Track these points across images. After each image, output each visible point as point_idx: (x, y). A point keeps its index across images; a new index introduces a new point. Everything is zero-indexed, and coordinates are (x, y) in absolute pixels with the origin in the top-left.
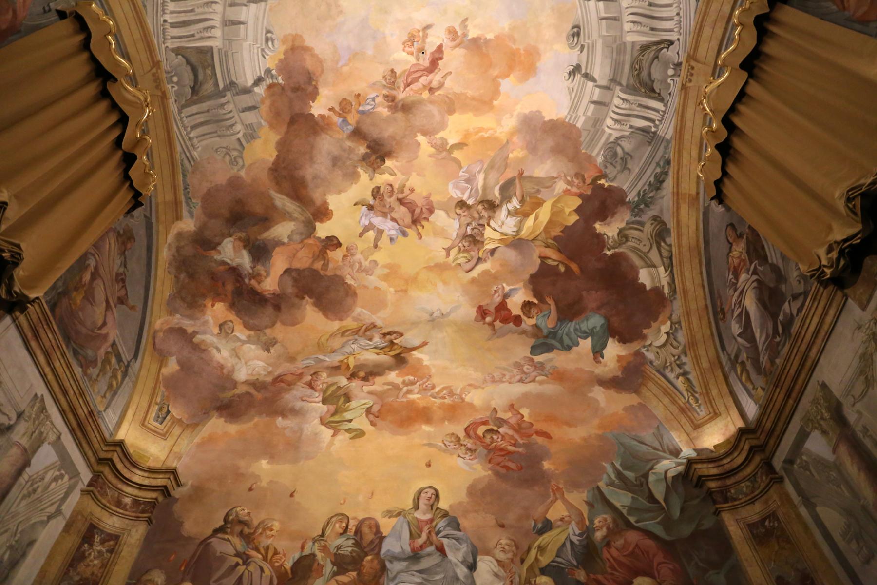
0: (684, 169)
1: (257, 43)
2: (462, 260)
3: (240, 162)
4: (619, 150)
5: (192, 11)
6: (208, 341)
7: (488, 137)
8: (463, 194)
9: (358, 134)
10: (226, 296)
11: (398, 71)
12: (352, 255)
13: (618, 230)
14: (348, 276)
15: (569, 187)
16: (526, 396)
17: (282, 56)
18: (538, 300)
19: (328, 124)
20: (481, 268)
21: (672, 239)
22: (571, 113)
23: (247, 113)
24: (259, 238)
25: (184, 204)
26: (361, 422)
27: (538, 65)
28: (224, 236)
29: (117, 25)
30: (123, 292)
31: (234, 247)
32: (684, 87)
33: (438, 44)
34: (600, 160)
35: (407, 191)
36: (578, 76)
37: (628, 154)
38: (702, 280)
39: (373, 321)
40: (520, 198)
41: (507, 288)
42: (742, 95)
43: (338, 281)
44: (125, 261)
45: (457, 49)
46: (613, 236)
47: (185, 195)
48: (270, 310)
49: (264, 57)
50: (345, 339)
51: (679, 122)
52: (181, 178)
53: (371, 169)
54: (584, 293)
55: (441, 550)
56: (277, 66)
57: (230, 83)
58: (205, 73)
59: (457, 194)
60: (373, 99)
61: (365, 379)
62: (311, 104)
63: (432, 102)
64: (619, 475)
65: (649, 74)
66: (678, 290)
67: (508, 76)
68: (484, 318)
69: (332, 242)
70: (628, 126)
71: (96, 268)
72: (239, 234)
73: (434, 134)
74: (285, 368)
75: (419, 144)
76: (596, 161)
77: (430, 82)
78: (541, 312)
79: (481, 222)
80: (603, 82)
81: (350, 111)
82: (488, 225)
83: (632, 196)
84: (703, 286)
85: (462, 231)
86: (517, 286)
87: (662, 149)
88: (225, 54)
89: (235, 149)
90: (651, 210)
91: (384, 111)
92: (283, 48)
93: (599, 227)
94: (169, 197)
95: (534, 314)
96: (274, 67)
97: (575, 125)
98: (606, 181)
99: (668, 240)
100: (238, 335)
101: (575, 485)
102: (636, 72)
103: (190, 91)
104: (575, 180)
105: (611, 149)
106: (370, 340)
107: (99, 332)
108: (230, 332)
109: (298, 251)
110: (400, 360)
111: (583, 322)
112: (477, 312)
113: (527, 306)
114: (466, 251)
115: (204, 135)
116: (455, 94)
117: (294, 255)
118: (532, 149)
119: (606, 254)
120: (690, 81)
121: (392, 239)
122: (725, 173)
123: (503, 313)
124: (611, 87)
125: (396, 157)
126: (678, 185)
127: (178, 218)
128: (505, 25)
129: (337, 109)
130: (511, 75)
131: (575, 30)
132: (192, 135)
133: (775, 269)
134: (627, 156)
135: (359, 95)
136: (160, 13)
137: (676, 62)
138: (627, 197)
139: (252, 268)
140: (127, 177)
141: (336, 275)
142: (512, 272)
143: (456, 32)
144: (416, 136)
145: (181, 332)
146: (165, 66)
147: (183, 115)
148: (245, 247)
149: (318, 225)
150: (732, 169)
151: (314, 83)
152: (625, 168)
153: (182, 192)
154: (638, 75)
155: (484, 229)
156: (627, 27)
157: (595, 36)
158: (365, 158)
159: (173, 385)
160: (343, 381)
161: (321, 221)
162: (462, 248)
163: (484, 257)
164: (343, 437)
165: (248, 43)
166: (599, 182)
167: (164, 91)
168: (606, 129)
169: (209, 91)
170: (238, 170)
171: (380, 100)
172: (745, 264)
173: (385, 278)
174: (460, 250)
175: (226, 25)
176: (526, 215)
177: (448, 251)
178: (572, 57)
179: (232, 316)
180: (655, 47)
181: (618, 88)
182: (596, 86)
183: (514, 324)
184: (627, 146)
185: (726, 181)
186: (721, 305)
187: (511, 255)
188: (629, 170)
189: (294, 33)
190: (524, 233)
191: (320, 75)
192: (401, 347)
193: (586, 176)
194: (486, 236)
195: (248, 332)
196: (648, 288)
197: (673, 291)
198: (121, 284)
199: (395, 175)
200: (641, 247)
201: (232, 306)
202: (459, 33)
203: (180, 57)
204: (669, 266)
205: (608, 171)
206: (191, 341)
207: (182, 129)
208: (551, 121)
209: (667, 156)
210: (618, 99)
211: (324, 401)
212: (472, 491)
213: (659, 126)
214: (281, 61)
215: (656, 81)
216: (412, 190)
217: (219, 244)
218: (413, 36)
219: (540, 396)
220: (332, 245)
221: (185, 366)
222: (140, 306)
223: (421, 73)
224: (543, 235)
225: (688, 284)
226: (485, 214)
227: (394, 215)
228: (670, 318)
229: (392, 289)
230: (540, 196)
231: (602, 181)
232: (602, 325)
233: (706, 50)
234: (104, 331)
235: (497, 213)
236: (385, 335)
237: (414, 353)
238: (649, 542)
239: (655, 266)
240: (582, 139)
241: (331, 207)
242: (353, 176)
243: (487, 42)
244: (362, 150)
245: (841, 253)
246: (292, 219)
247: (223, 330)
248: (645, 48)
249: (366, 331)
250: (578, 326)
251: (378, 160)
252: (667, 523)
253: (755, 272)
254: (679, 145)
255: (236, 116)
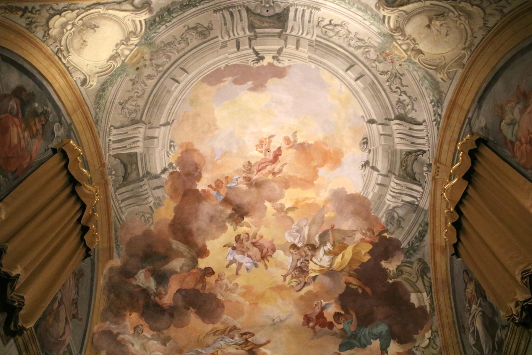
0: (437, 229)
1: (164, 148)
2: (294, 284)
3: (151, 220)
4: (395, 215)
5: (126, 133)
6: (126, 339)
7: (311, 204)
8: (295, 239)
9: (227, 201)
10: (139, 308)
11: (253, 162)
12: (222, 280)
13: (396, 267)
14: (219, 294)
15: (364, 237)
17: (179, 155)
18: (344, 311)
19: (207, 195)
20: (306, 289)
21: (431, 275)
22: (364, 190)
23: (157, 190)
24: (161, 269)
25: (115, 249)
27: (342, 160)
28: (139, 269)
29: (83, 151)
30: (75, 312)
31: (145, 276)
32: (434, 179)
33: (279, 146)
34: (383, 220)
35: (258, 238)
36: (368, 168)
37: (401, 217)
38: (451, 304)
39: (235, 324)
40: (332, 243)
41: (324, 303)
42: (465, 194)
43: (212, 297)
44: (78, 290)
45: (291, 149)
46: (393, 271)
47: (116, 243)
48: (166, 317)
49: (168, 156)
50: (216, 337)
51: (432, 200)
52: (114, 233)
53: (234, 223)
54: (375, 308)
56: (176, 161)
57: (147, 173)
58: (131, 169)
59: (290, 240)
60: (237, 180)
62: (197, 183)
63: (274, 181)
65: (412, 170)
66: (435, 309)
67: (323, 166)
68: (308, 323)
69: (209, 271)
70: (400, 200)
71: (61, 298)
72: (148, 267)
73: (276, 201)
75: (266, 208)
76: (381, 220)
77: (274, 169)
78: (347, 320)
79: (307, 258)
80: (384, 172)
81: (222, 187)
82: (311, 260)
83: (404, 245)
84: (452, 308)
85: (294, 264)
86: (330, 302)
87: (422, 216)
88: (144, 156)
89: (148, 213)
90: (418, 254)
91: (244, 187)
92: (180, 151)
93: (383, 264)
94: (106, 245)
95: (342, 322)
96: (174, 162)
97: (367, 198)
98: (388, 234)
99: (428, 275)
100: (145, 333)
102: (404, 168)
103: (122, 178)
104: (368, 233)
105: (391, 213)
106: (233, 338)
107: (60, 339)
108: (140, 332)
109: (186, 277)
111: (374, 327)
112: (304, 319)
113: (337, 315)
114: (296, 277)
115: (129, 205)
116: (289, 176)
117: (184, 280)
118: (340, 211)
119: (388, 282)
120: (438, 175)
121: (248, 269)
122: (459, 240)
123: (321, 320)
124: (389, 175)
125: (251, 216)
126: (434, 240)
127: (111, 258)
128: (320, 136)
129: (214, 186)
130: (325, 166)
131: (365, 140)
132: (121, 205)
133: (491, 306)
134: (400, 219)
135: (227, 177)
136: (107, 135)
137: (428, 163)
138: (401, 245)
139: (156, 289)
140: (82, 240)
141: (211, 294)
142: (328, 292)
143: (290, 140)
144: (264, 202)
145: (109, 333)
146: (108, 166)
147: (117, 193)
148: (152, 275)
149: (199, 260)
150: (462, 238)
151: (199, 170)
152: (399, 226)
153: (114, 241)
154: (405, 169)
155: (309, 263)
156: (397, 140)
157: (377, 144)
158: (231, 217)
161: (202, 257)
162: (294, 276)
163: (308, 282)
165: (159, 149)
166: (383, 235)
167: (107, 180)
168: (387, 201)
169: (134, 178)
170: (150, 226)
171: (241, 180)
172: (474, 299)
173: (243, 295)
174: (292, 277)
175: (146, 139)
176: (336, 255)
177: (285, 277)
178: (364, 156)
179: (142, 322)
180: (415, 154)
181: (393, 176)
182: (379, 174)
183: (329, 328)
184: (401, 212)
185: (460, 244)
186: (463, 323)
187: (326, 281)
188: (403, 228)
189: (187, 142)
190: (335, 266)
191: (203, 166)
192: (253, 344)
193: (375, 230)
194: (310, 268)
195: (152, 333)
196: (416, 306)
197: (433, 309)
198: (75, 306)
199: (251, 227)
200: (411, 278)
201: (143, 315)
202: (292, 140)
203: (117, 159)
204: (430, 293)
205: (389, 228)
206: (116, 340)
207: (116, 202)
208: (352, 194)
209: (426, 220)
210: (393, 183)
213: (420, 201)
214: (179, 158)
215: (416, 174)
216: (262, 237)
217: (136, 274)
218: (262, 142)
220: (208, 273)
222: (85, 318)
223: (268, 164)
224: (347, 268)
225: (442, 305)
226: (309, 253)
227: (250, 253)
228: (431, 328)
229: (247, 303)
230: (345, 242)
231: (385, 234)
232: (387, 331)
233: (446, 157)
234: (63, 338)
235: (317, 253)
236: (242, 335)
237: (261, 348)
239: (420, 292)
240: (372, 207)
241: (208, 248)
242: (223, 228)
243: (310, 145)
244: (229, 211)
245: (523, 308)
246: (182, 256)
247: (136, 331)
248: (408, 153)
249: (230, 331)
250: (371, 331)
251: (240, 218)
253: (480, 306)
254: (433, 214)
255: (150, 192)
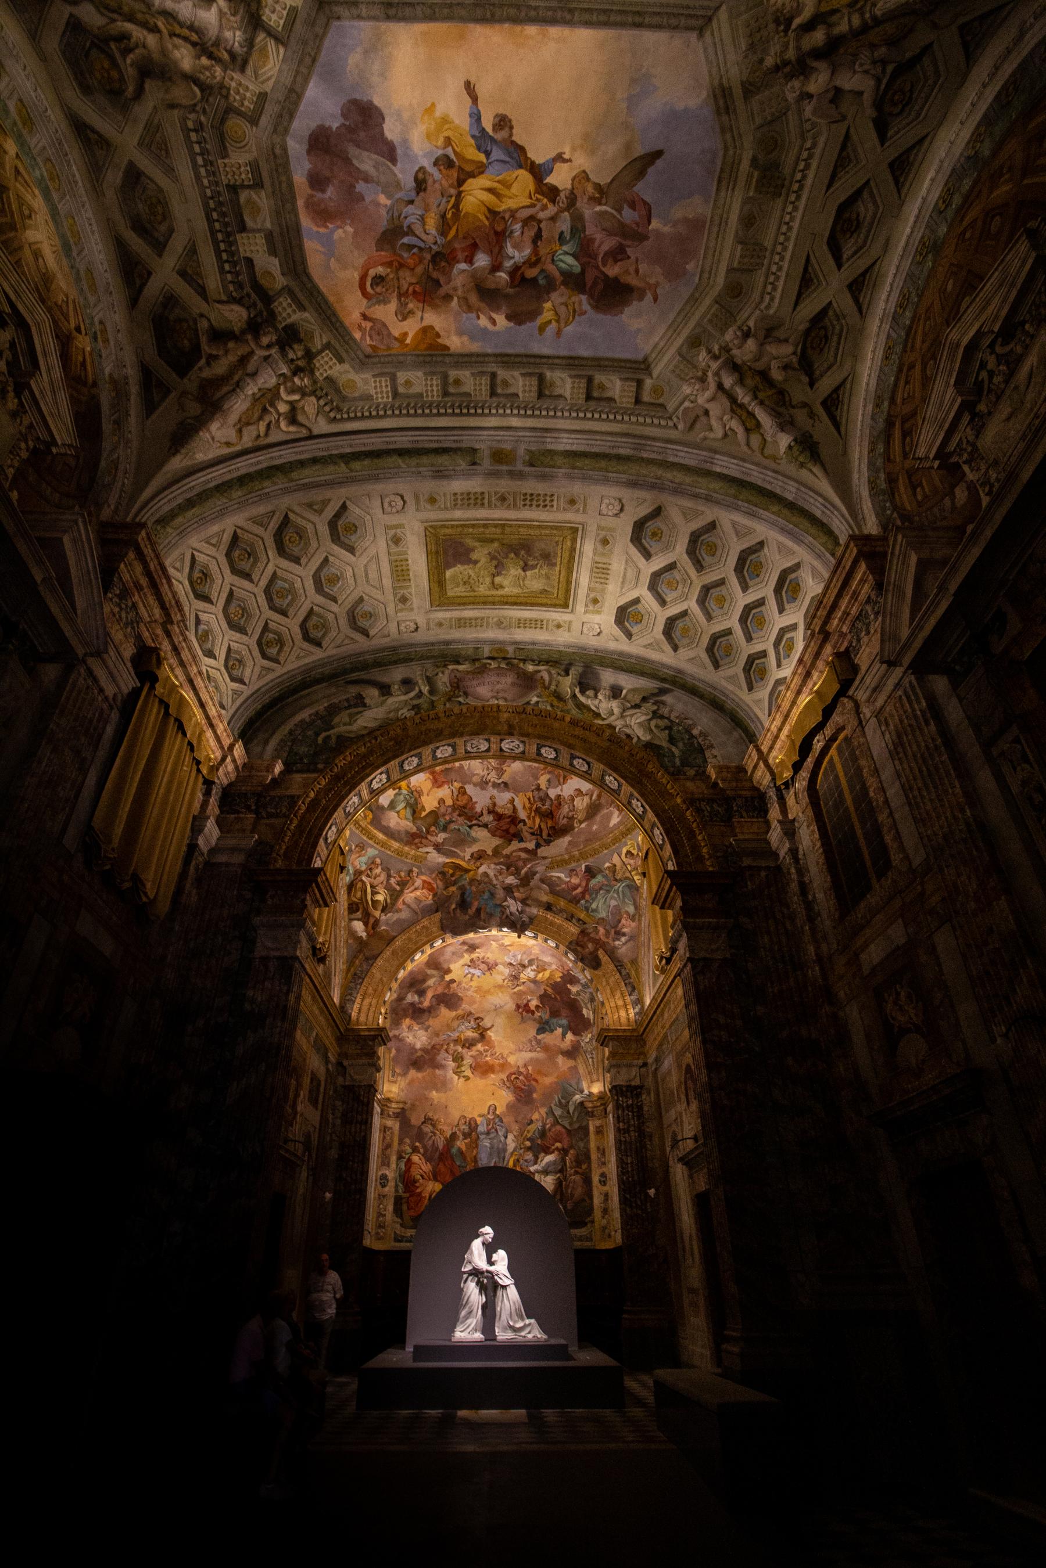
16: (531, 1059)
20: (518, 988)
26: (468, 1072)
48: (427, 1014)
55: (496, 1131)
59: (508, 960)
61: (468, 1048)
64: (560, 1101)
69: (453, 981)
74: (435, 1040)
101: (543, 1105)
110: (483, 1037)
113: (537, 1007)
142: (532, 992)
158: (467, 950)
159: (395, 1060)
160: (460, 1049)
164: (462, 1080)
173: (476, 992)
187: (532, 985)
201: (412, 1018)
204: (594, 1013)
211: (454, 1061)
212: (507, 1106)
219: (537, 1060)
221: (398, 1050)
238: (563, 1130)
242: (462, 956)
244: (466, 948)
252: (571, 1124)
